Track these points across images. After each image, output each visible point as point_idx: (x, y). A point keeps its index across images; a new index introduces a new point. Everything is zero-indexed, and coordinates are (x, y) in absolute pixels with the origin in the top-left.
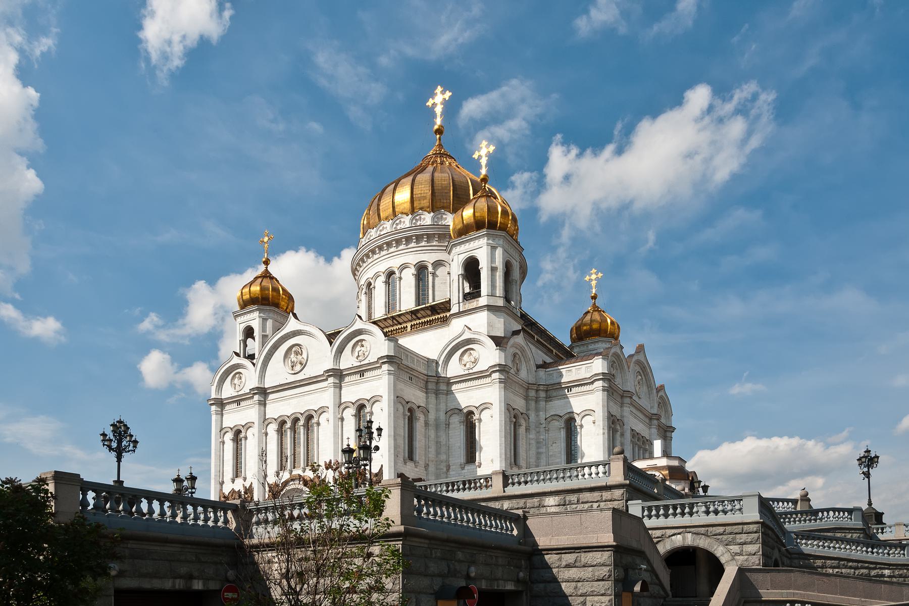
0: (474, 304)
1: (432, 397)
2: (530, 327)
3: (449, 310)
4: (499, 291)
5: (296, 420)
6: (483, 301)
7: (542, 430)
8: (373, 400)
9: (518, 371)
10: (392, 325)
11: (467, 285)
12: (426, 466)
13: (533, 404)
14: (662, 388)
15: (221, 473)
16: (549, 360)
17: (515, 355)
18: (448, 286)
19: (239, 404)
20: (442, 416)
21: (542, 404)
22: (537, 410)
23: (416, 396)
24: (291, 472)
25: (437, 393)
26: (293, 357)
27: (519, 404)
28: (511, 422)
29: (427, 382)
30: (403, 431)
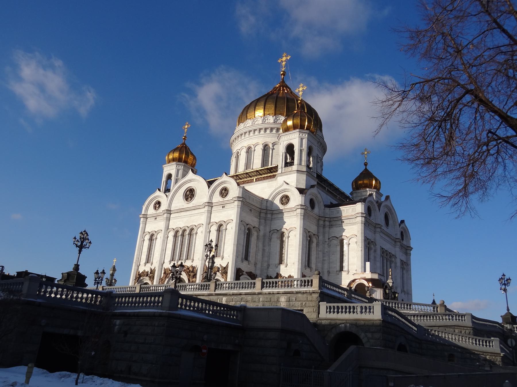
0: (289, 168)
4: (304, 163)
5: (184, 231)
6: (295, 167)
7: (326, 246)
8: (228, 222)
11: (288, 157)
12: (255, 264)
13: (321, 230)
14: (403, 222)
15: (139, 259)
16: (335, 202)
18: (278, 158)
19: (156, 219)
21: (327, 229)
22: (324, 233)
23: (253, 221)
25: (265, 219)
27: (313, 229)
28: (307, 240)
29: (260, 212)
30: (243, 242)
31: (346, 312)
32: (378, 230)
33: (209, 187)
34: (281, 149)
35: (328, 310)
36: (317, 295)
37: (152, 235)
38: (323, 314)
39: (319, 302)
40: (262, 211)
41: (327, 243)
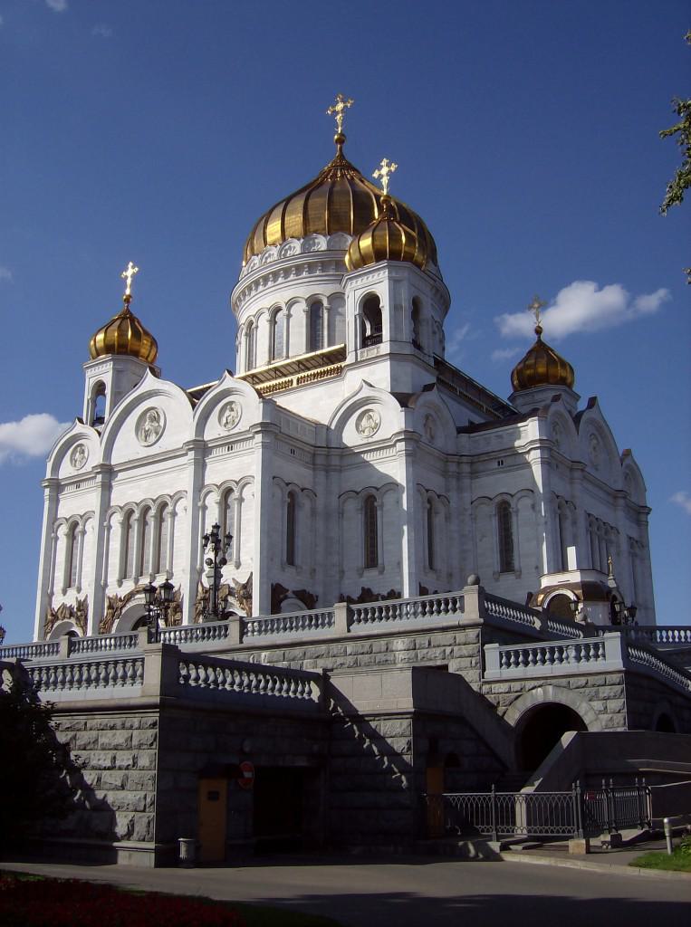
0: (372, 351)
1: (321, 476)
2: (448, 378)
3: (345, 359)
5: (147, 509)
6: (385, 348)
9: (432, 437)
10: (268, 383)
11: (368, 326)
13: (454, 482)
14: (628, 453)
15: (49, 580)
16: (478, 420)
17: (427, 417)
20: (334, 499)
21: (467, 481)
22: (460, 490)
23: (299, 474)
24: (137, 581)
25: (328, 469)
26: (147, 426)
27: (436, 482)
28: (424, 508)
30: (283, 526)
31: (544, 662)
32: (577, 474)
33: (194, 405)
34: (352, 309)
35: (504, 660)
36: (478, 630)
37: (74, 525)
38: (493, 671)
39: (483, 645)
40: (319, 451)
41: (469, 512)
